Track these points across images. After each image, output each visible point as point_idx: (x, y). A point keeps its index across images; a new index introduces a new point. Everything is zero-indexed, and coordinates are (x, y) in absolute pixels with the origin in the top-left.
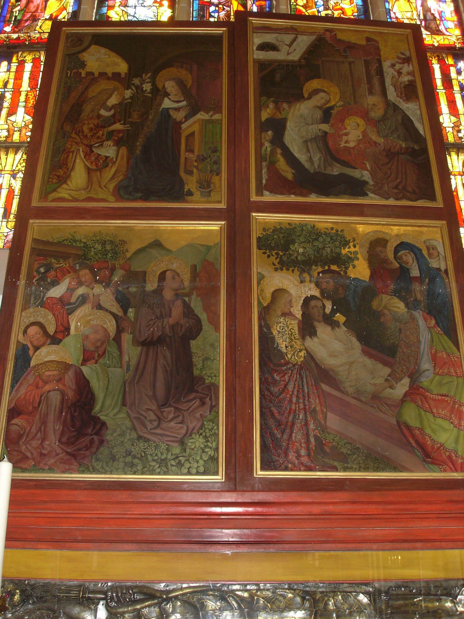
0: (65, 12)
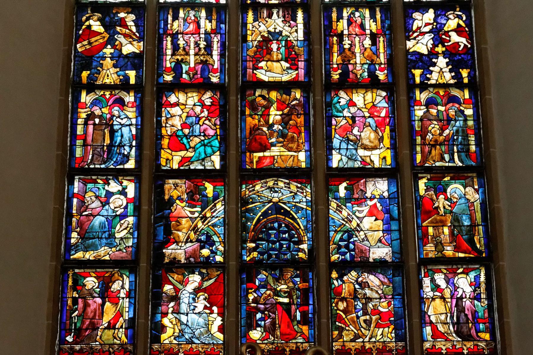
0: (121, 318)
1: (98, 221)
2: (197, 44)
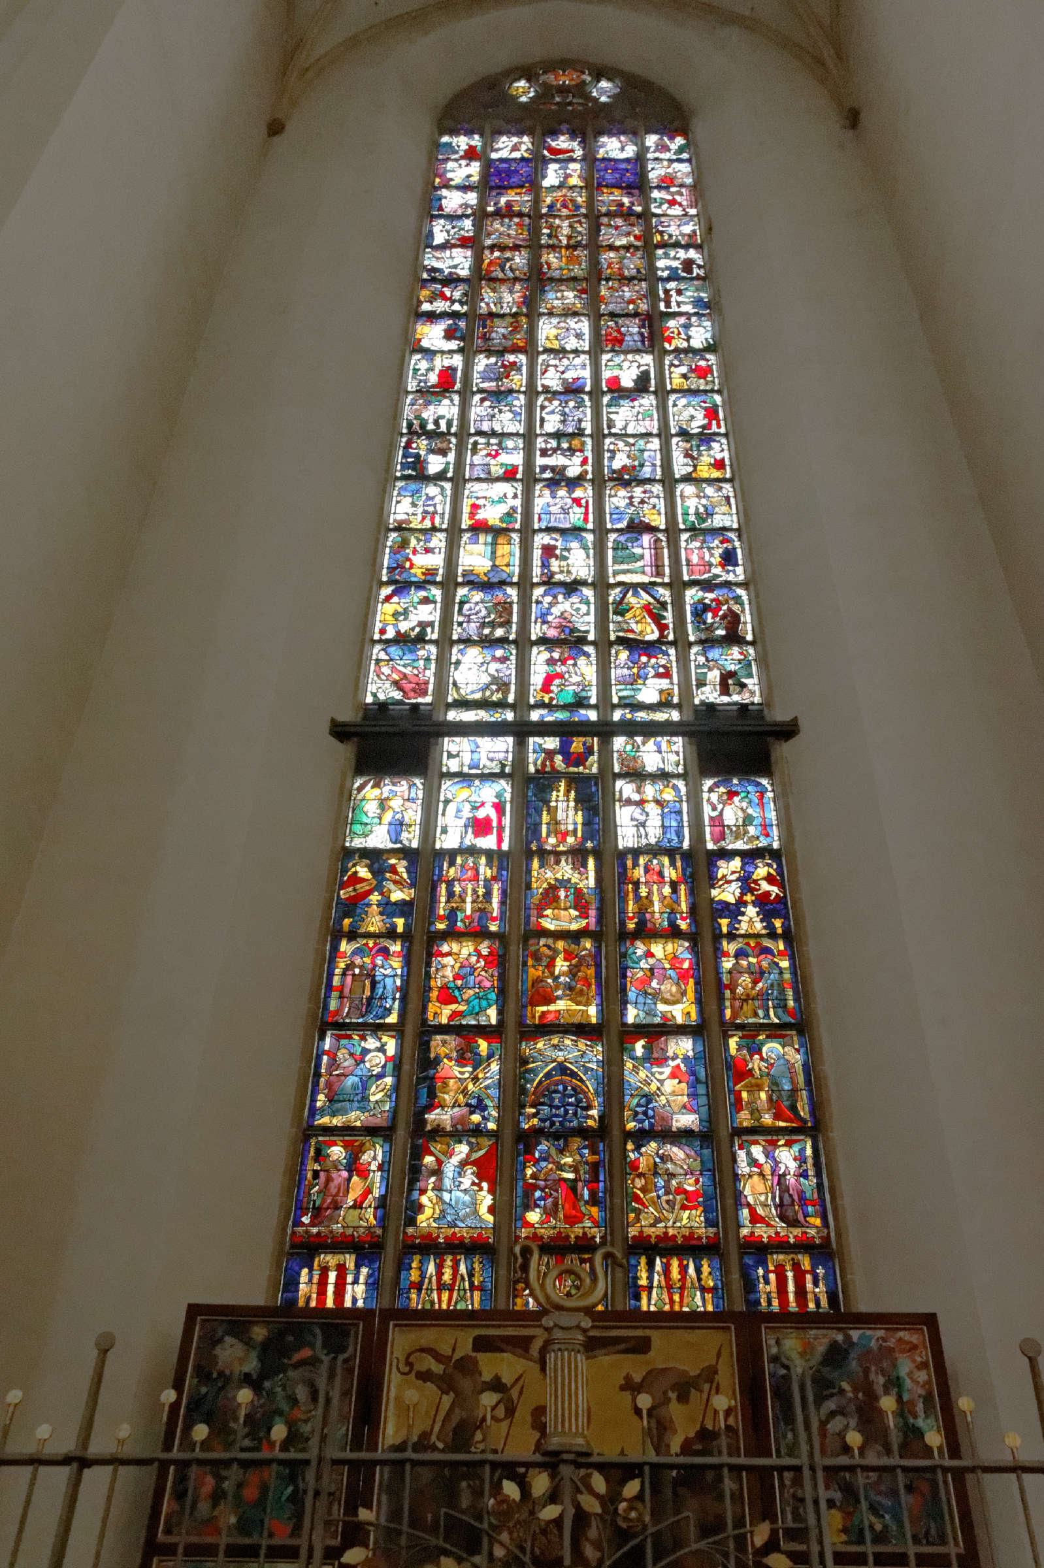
1: (351, 1080)
2: (475, 891)
